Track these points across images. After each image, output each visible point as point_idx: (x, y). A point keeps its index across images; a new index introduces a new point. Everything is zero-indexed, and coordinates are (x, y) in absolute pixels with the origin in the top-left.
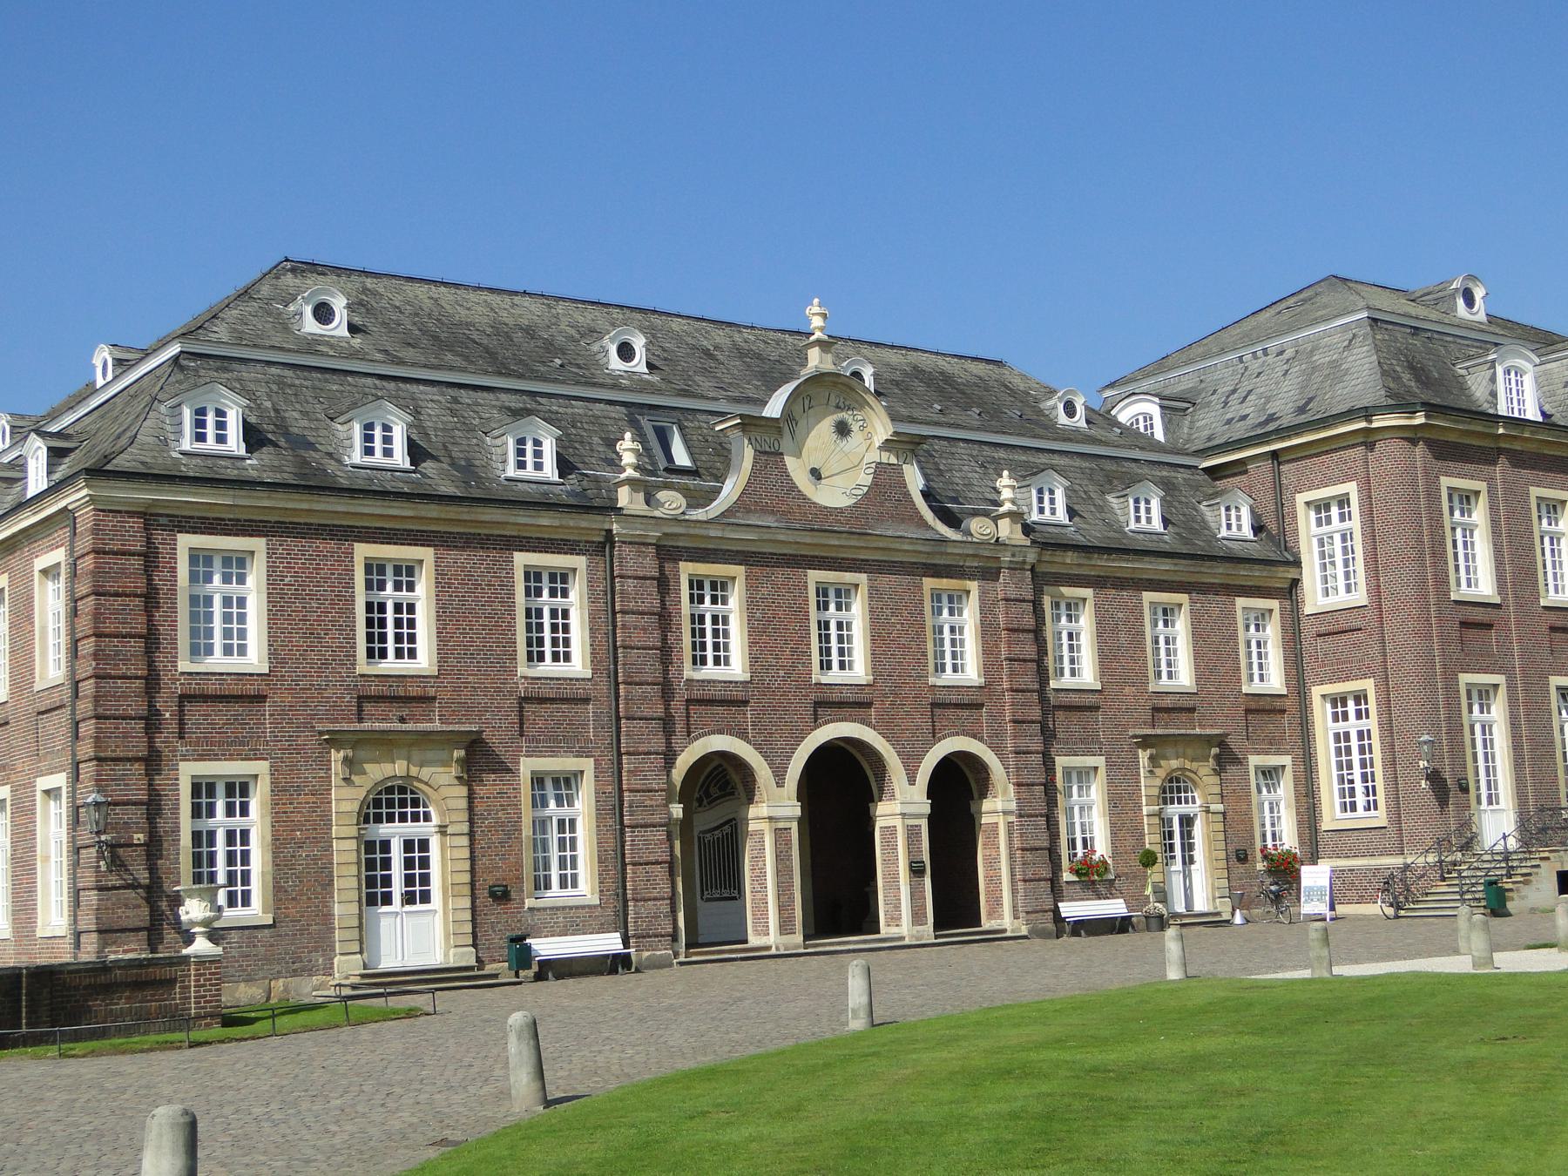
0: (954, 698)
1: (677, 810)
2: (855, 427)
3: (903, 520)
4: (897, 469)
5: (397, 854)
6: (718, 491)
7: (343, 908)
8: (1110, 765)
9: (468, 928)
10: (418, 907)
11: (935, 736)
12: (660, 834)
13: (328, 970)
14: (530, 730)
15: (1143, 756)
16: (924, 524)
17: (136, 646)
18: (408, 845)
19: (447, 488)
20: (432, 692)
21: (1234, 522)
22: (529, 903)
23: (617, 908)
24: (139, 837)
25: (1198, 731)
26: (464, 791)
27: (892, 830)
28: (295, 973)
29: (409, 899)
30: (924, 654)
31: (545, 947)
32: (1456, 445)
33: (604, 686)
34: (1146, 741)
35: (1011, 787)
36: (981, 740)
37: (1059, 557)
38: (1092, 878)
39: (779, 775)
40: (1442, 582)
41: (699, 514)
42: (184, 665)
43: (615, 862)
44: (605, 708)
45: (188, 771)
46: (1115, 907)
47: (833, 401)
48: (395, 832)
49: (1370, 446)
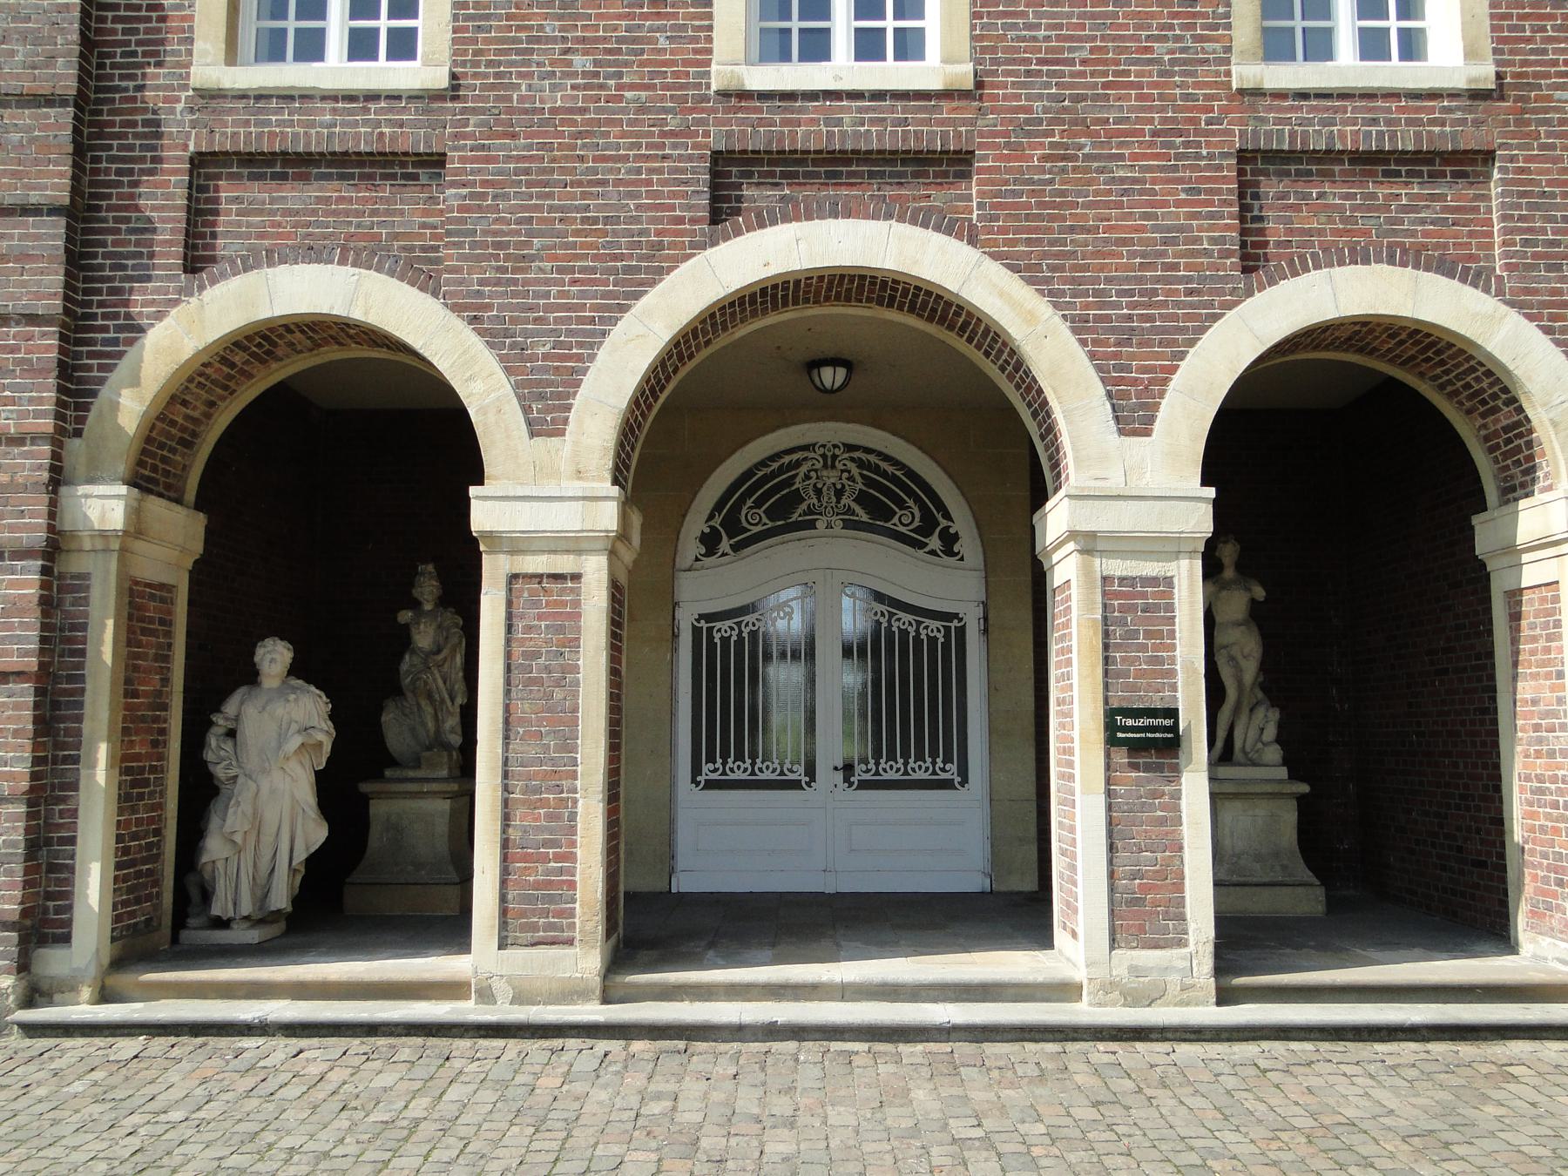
0: (1349, 133)
11: (1255, 261)
36: (1478, 278)
39: (546, 411)
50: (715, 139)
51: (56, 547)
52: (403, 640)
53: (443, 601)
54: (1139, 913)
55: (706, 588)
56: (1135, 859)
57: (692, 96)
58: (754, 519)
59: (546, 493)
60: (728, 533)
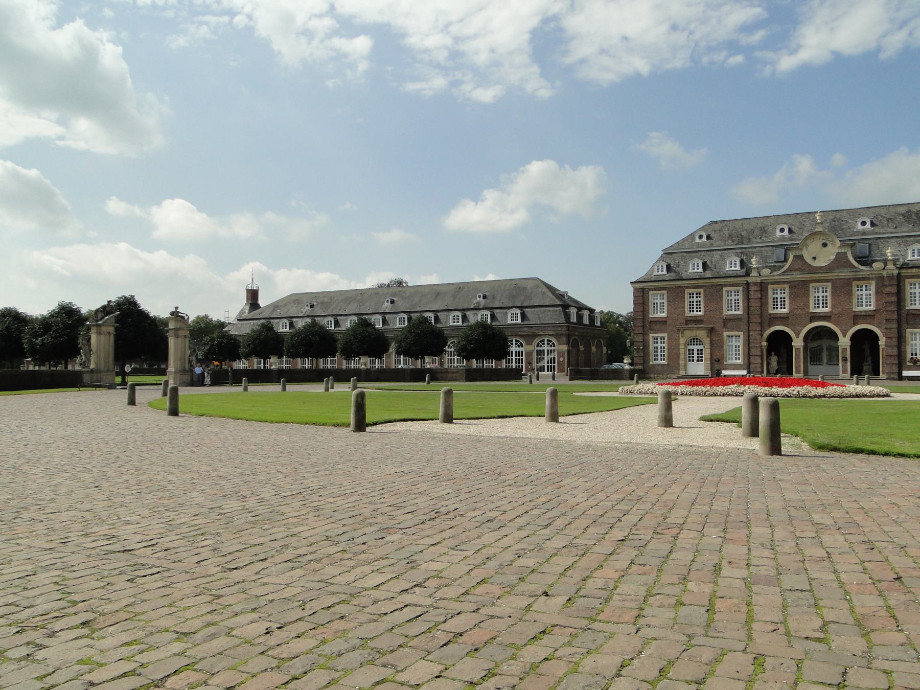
1: (765, 344)
2: (829, 244)
4: (845, 253)
5: (695, 352)
7: (682, 362)
11: (855, 324)
16: (854, 267)
19: (708, 276)
23: (748, 366)
31: (724, 372)
33: (746, 316)
37: (909, 271)
41: (775, 273)
43: (748, 355)
45: (651, 335)
48: (695, 348)
54: (844, 371)
56: (844, 368)
57: (808, 312)
59: (798, 343)
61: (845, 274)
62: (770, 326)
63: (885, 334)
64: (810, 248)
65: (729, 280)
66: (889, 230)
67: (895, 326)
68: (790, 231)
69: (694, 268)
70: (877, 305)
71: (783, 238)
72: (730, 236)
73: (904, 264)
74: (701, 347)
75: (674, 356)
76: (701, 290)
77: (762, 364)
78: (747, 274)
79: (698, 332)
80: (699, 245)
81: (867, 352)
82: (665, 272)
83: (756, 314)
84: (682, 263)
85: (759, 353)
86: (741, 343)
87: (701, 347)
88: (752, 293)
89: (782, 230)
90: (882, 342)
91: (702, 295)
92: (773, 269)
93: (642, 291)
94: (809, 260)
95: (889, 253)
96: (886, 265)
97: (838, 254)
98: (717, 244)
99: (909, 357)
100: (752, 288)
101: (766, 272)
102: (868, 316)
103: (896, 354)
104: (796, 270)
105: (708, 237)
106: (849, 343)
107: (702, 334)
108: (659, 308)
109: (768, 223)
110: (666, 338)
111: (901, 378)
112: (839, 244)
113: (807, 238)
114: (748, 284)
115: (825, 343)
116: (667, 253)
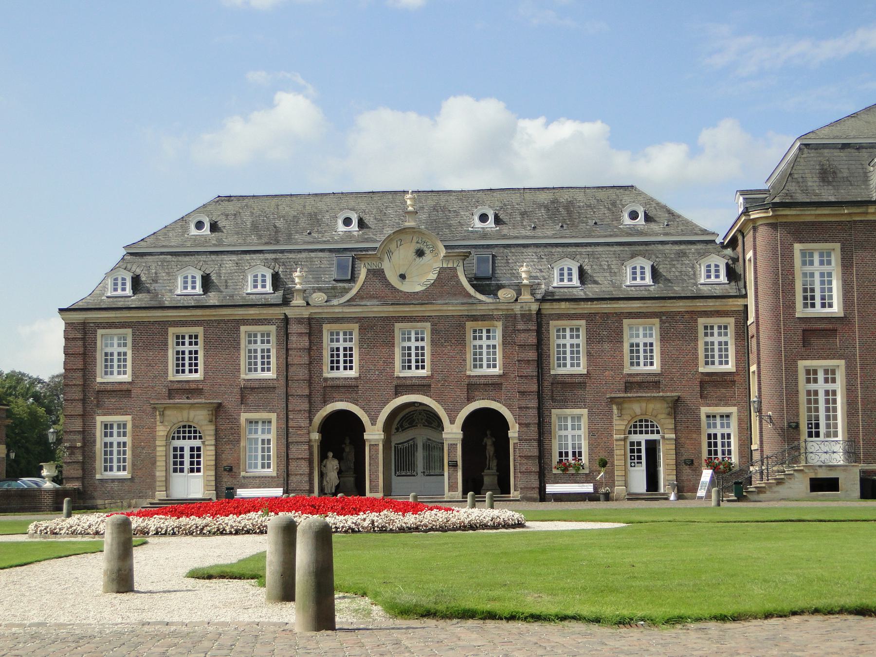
1: (316, 436)
2: (427, 251)
3: (455, 295)
5: (187, 453)
6: (350, 289)
7: (160, 474)
8: (590, 414)
9: (213, 483)
10: (196, 474)
11: (470, 400)
12: (307, 447)
13: (153, 497)
14: (249, 402)
15: (615, 407)
16: (470, 296)
17: (80, 374)
18: (192, 449)
19: (212, 302)
20: (201, 387)
21: (710, 274)
22: (243, 474)
23: (285, 479)
24: (79, 444)
25: (661, 394)
26: (213, 427)
27: (374, 446)
28: (140, 497)
29: (192, 470)
30: (465, 360)
32: (813, 223)
33: (283, 382)
34: (612, 400)
35: (517, 425)
37: (556, 305)
38: (569, 472)
39: (374, 422)
40: (791, 306)
41: (335, 302)
42: (99, 380)
43: (286, 459)
44: (281, 391)
45: (100, 419)
46: (589, 488)
47: (415, 240)
48: (187, 444)
49: (755, 229)
50: (395, 383)
51: (310, 441)
52: (343, 450)
53: (350, 443)
55: (399, 438)
56: (452, 480)
57: (392, 378)
58: (406, 425)
59: (374, 434)
60: (401, 428)
61: (452, 308)
62: (325, 402)
63: (518, 418)
64: (395, 256)
65: (252, 311)
66: (524, 232)
67: (534, 403)
68: (362, 224)
69: (184, 285)
70: (505, 366)
71: (349, 236)
72: (255, 227)
73: (547, 293)
74: (196, 443)
75: (143, 463)
76: (199, 330)
77: (311, 474)
78: (286, 302)
79: (192, 413)
80: (195, 238)
81: (490, 450)
82: (129, 291)
83: (302, 380)
84: (163, 274)
85: (306, 455)
86: (272, 436)
87: (196, 443)
88: (293, 338)
89: (347, 222)
90: (513, 433)
91: (200, 340)
92: (332, 293)
93: (82, 330)
94: (392, 278)
95: (524, 272)
96: (519, 293)
97: (442, 270)
98: (230, 240)
99: (556, 458)
100: (294, 328)
101: (319, 298)
102: (491, 386)
103: (536, 453)
104: (372, 297)
105: (214, 227)
106: (461, 436)
107: (200, 418)
108: (117, 362)
109: (322, 206)
110: (129, 426)
111: (543, 497)
112: (443, 252)
113: (390, 239)
114: (286, 320)
115: (420, 435)
116: (135, 253)
